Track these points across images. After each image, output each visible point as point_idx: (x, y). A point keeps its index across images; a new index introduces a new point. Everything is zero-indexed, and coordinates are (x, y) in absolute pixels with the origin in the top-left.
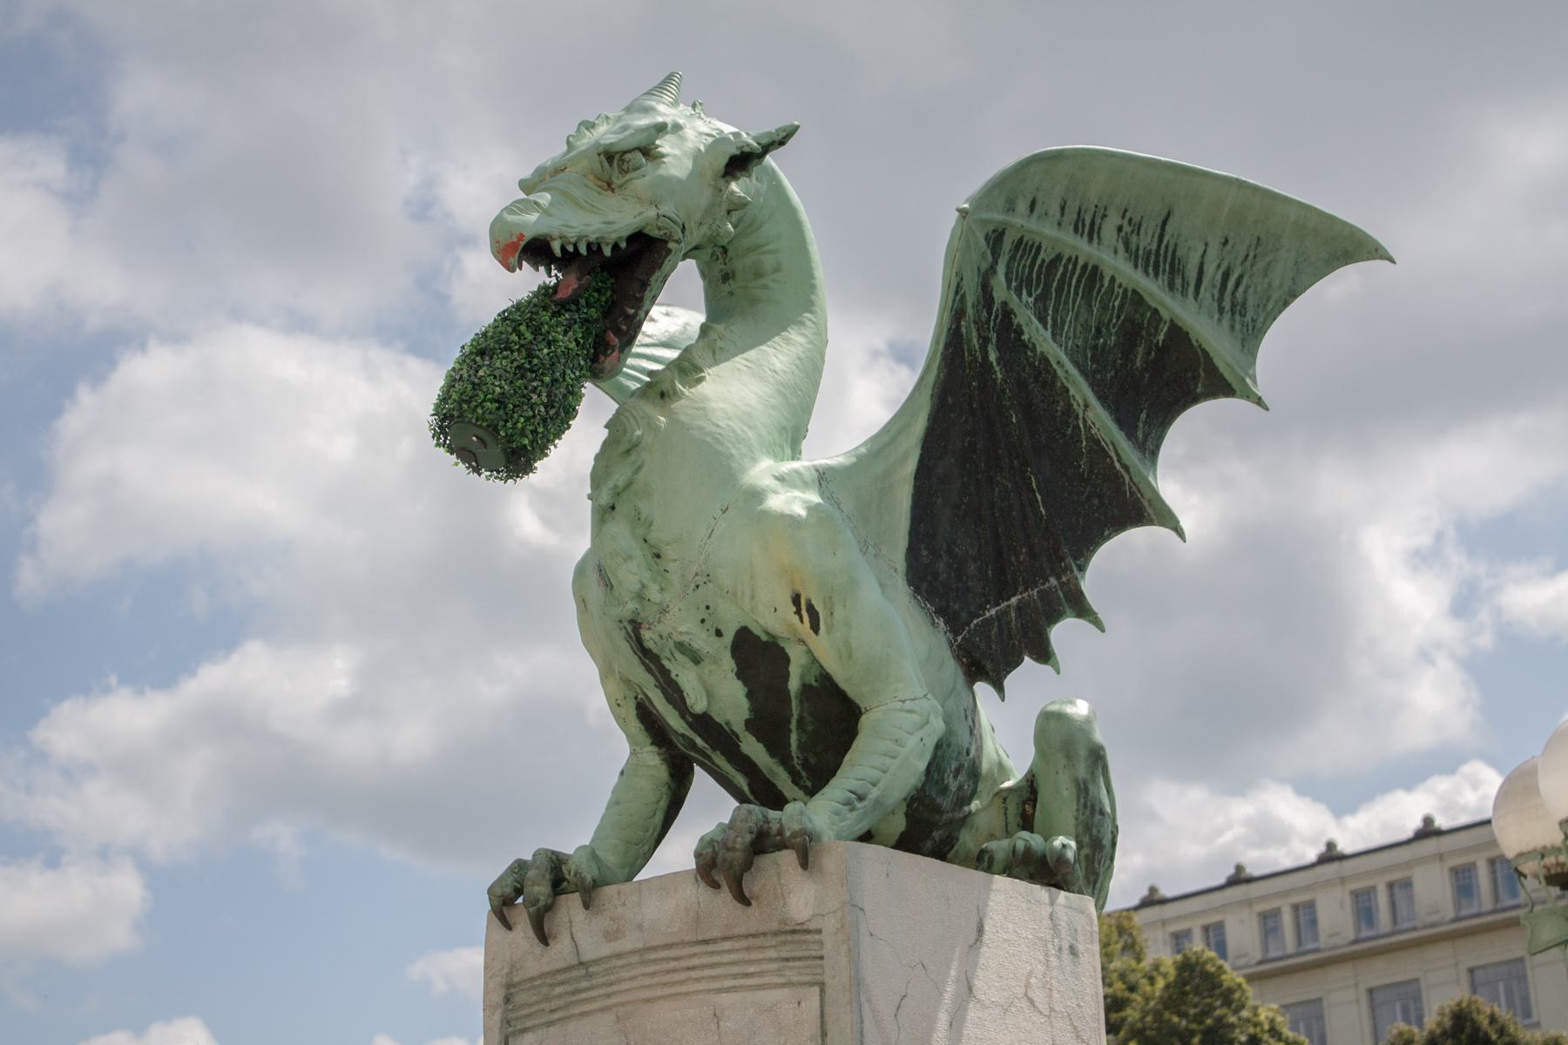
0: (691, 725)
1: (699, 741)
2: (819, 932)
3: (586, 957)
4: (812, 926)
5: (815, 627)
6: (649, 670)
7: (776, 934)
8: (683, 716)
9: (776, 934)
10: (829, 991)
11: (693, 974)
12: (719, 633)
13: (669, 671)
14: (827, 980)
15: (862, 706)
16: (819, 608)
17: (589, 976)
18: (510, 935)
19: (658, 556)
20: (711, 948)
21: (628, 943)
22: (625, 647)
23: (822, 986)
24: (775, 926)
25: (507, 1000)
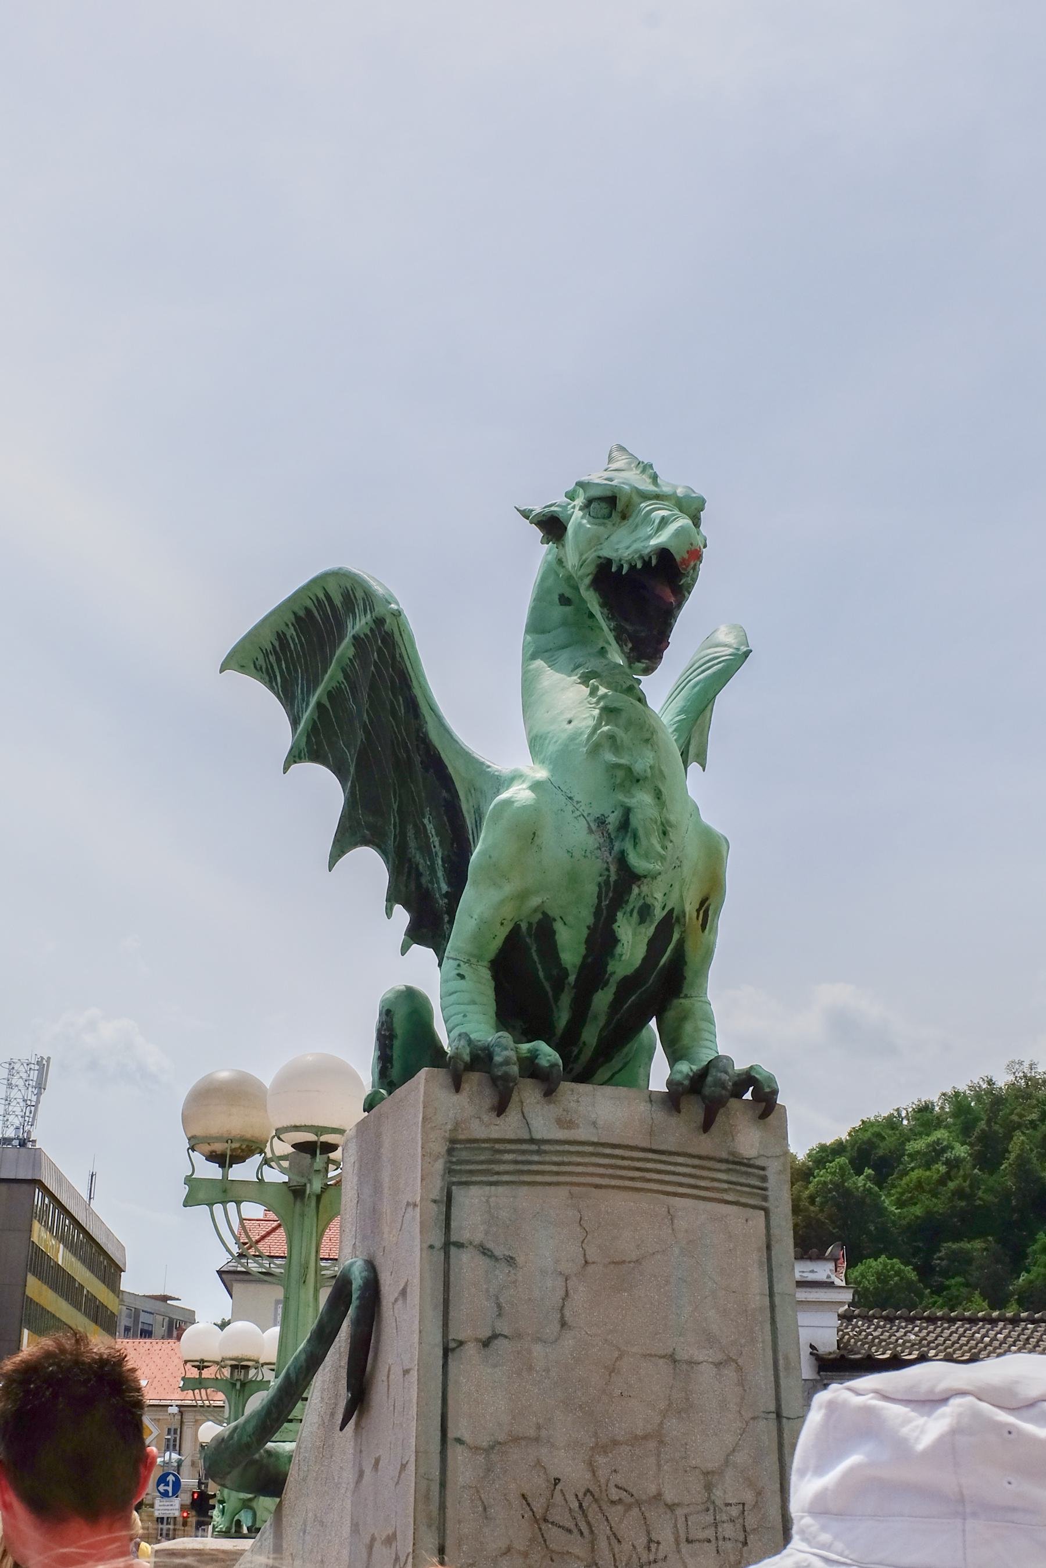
0: (584, 967)
1: (572, 978)
2: (763, 1169)
3: (537, 1136)
4: (760, 1162)
5: (704, 926)
6: (597, 913)
7: (727, 1161)
8: (585, 957)
9: (727, 1161)
10: (773, 1217)
11: (648, 1175)
12: (663, 909)
13: (616, 921)
14: (772, 1208)
15: (685, 991)
16: (710, 913)
17: (538, 1152)
18: (455, 1098)
19: (665, 833)
20: (664, 1158)
21: (582, 1133)
22: (590, 890)
23: (766, 1210)
24: (724, 1155)
25: (450, 1151)
